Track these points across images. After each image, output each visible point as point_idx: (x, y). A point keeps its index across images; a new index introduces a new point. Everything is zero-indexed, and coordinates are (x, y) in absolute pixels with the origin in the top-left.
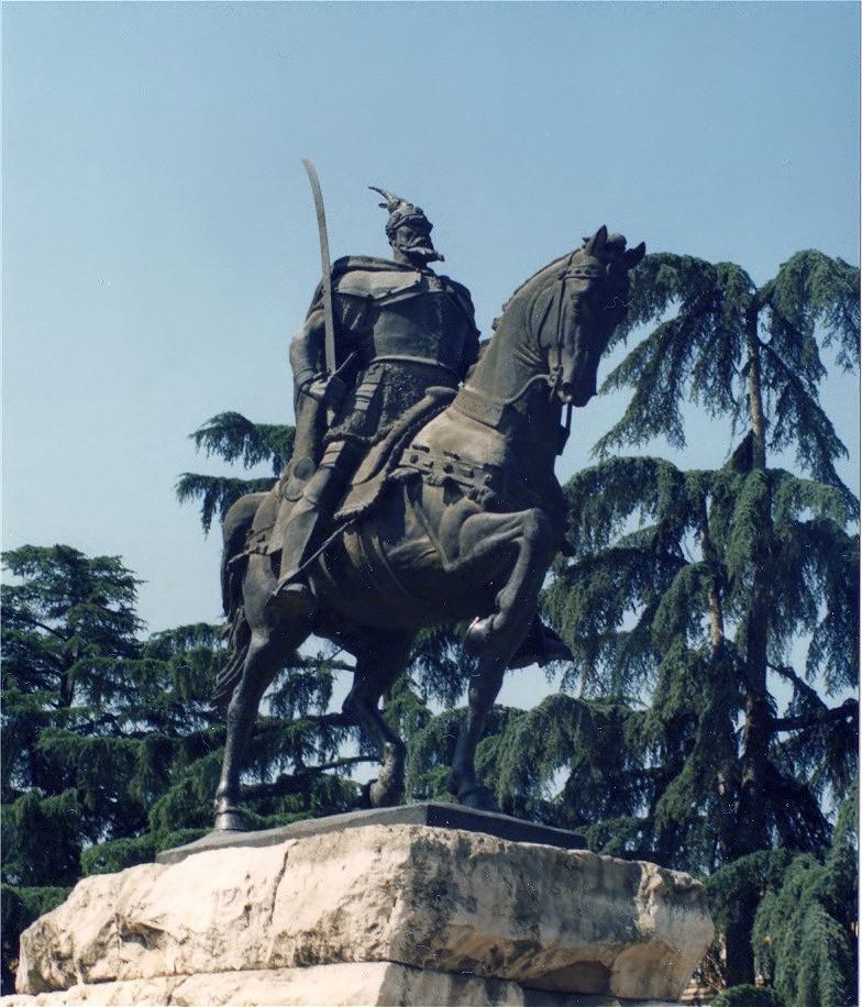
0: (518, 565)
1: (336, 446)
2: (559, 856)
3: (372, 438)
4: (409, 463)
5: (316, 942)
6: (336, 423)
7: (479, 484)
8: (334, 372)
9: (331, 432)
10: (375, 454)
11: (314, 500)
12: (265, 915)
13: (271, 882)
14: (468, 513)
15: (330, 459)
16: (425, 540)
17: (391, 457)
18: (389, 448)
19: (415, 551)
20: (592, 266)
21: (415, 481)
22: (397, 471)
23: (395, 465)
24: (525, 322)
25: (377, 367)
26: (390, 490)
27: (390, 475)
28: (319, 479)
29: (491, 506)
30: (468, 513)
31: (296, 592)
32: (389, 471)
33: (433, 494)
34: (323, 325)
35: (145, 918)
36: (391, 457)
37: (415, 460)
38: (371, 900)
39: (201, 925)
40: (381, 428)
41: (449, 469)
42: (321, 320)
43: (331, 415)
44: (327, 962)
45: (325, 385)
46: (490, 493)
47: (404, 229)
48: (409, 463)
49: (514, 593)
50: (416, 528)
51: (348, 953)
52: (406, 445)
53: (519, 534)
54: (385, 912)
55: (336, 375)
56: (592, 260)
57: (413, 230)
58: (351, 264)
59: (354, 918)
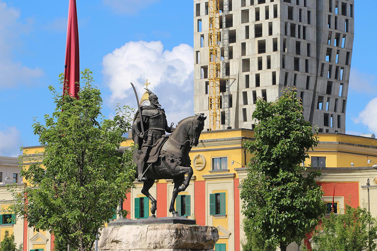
3: (153, 146)
6: (145, 143)
9: (143, 145)
10: (154, 149)
11: (143, 159)
12: (145, 239)
13: (145, 234)
19: (164, 170)
20: (199, 122)
21: (164, 159)
24: (185, 129)
27: (160, 156)
29: (181, 165)
33: (168, 161)
34: (140, 121)
35: (118, 239)
39: (131, 241)
42: (139, 120)
44: (160, 248)
47: (153, 100)
54: (171, 240)
56: (198, 121)
57: (154, 99)
58: (143, 108)
59: (166, 241)
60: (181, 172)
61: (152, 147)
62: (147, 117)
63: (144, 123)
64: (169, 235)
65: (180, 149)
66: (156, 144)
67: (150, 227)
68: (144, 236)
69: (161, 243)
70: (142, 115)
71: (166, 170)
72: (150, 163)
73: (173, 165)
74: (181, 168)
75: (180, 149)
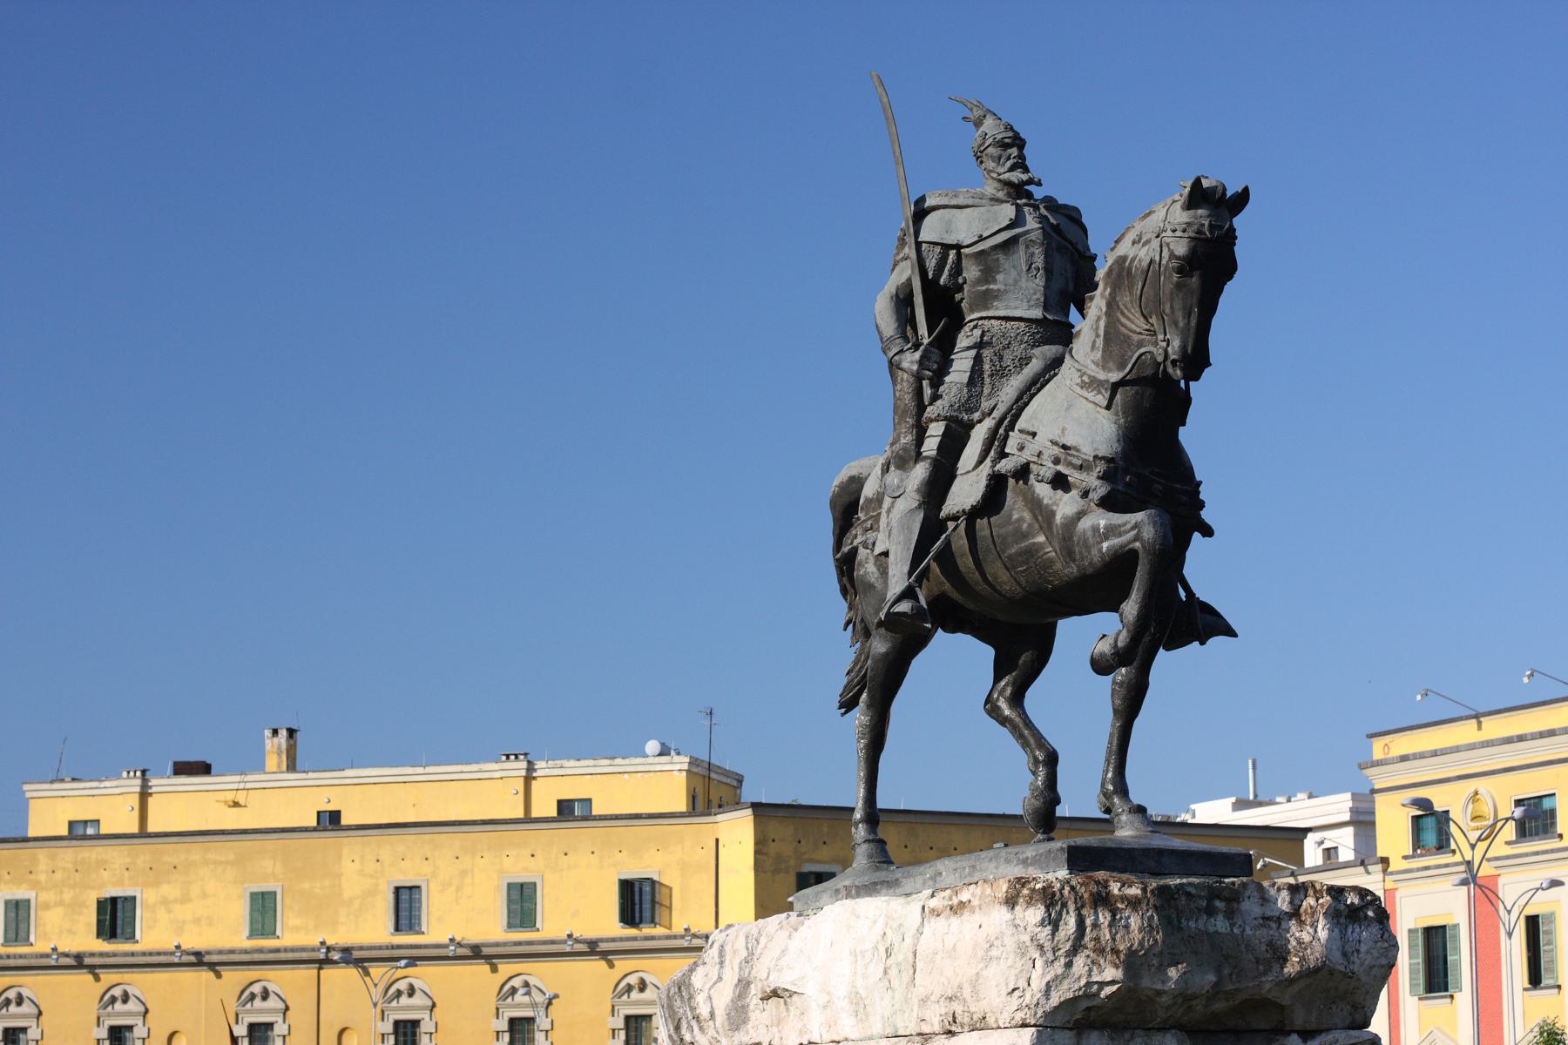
0: (1138, 575)
1: (936, 430)
2: (1210, 887)
3: (976, 416)
4: (1015, 451)
5: (957, 1007)
6: (935, 397)
7: (1091, 480)
8: (926, 341)
9: (931, 411)
10: (979, 435)
11: (917, 497)
12: (906, 976)
14: (1080, 515)
15: (931, 446)
16: (1041, 539)
17: (996, 444)
18: (993, 433)
21: (1023, 472)
22: (1004, 461)
23: (1003, 455)
25: (975, 327)
26: (997, 485)
28: (920, 472)
29: (1107, 503)
30: (1080, 515)
31: (904, 614)
32: (995, 462)
34: (909, 280)
36: (996, 444)
37: (1021, 448)
38: (1010, 962)
40: (986, 405)
41: (1057, 461)
43: (927, 392)
45: (917, 355)
46: (1101, 490)
47: (991, 150)
48: (1015, 451)
49: (1136, 607)
50: (1030, 525)
51: (991, 1021)
52: (1011, 427)
53: (1136, 539)
55: (930, 344)
58: (929, 203)
60: (1105, 545)
61: (971, 426)
62: (946, 247)
63: (929, 285)
64: (1010, 942)
65: (1108, 407)
66: (992, 402)
67: (933, 903)
68: (902, 954)
69: (967, 992)
70: (918, 245)
71: (1040, 546)
72: (955, 518)
73: (1065, 505)
74: (1102, 519)
75: (1108, 407)
